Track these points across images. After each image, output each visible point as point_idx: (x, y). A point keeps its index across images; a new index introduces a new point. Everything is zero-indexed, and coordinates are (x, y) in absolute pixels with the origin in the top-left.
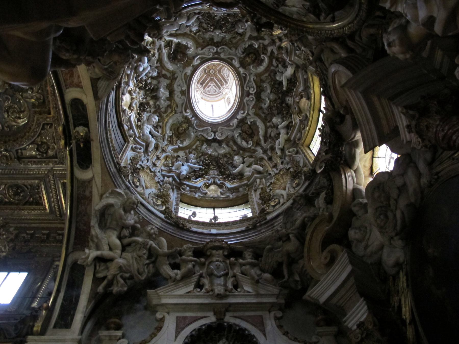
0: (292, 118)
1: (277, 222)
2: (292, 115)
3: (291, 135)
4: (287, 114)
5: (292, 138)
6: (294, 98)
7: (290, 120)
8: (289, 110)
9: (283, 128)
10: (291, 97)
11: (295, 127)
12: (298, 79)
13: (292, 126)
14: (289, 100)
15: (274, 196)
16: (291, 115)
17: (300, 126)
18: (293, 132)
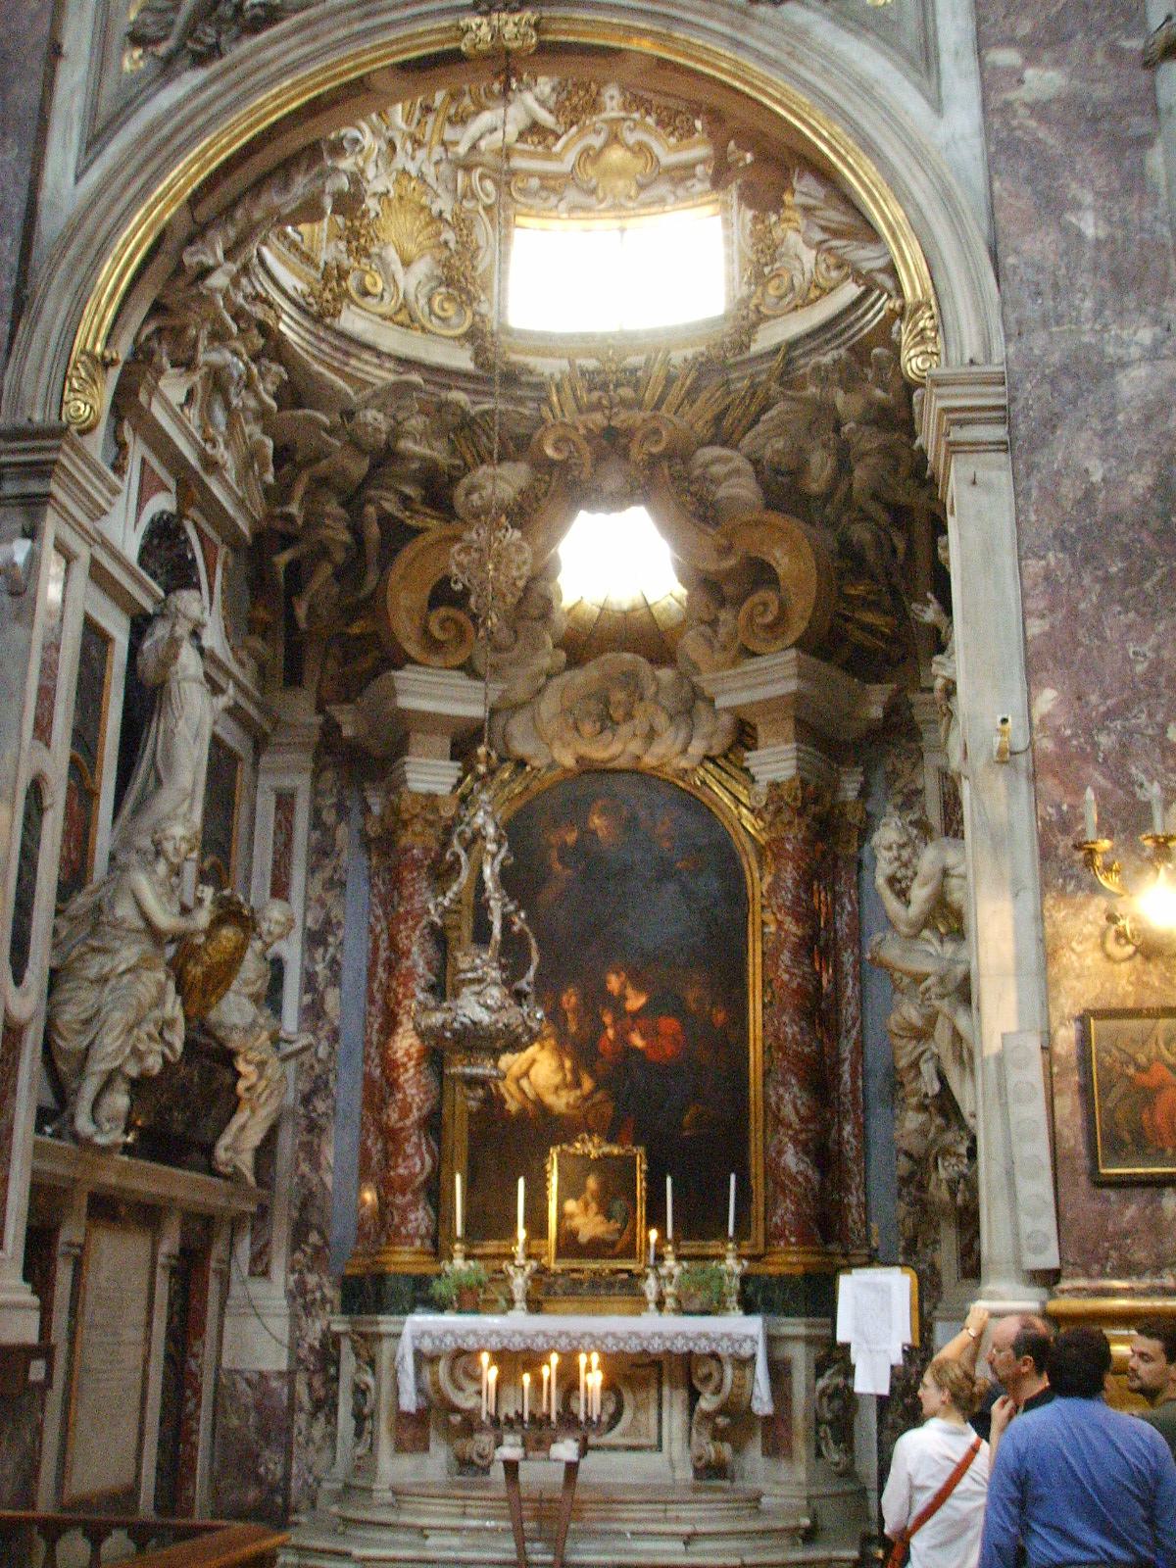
0: (566, 132)
1: (359, 359)
2: (574, 129)
3: (523, 153)
4: (574, 109)
5: (517, 163)
6: (624, 119)
7: (560, 130)
8: (584, 111)
9: (528, 111)
10: (625, 107)
11: (548, 155)
12: (685, 142)
13: (548, 148)
14: (612, 98)
15: (380, 256)
16: (572, 124)
17: (556, 176)
18: (532, 155)
